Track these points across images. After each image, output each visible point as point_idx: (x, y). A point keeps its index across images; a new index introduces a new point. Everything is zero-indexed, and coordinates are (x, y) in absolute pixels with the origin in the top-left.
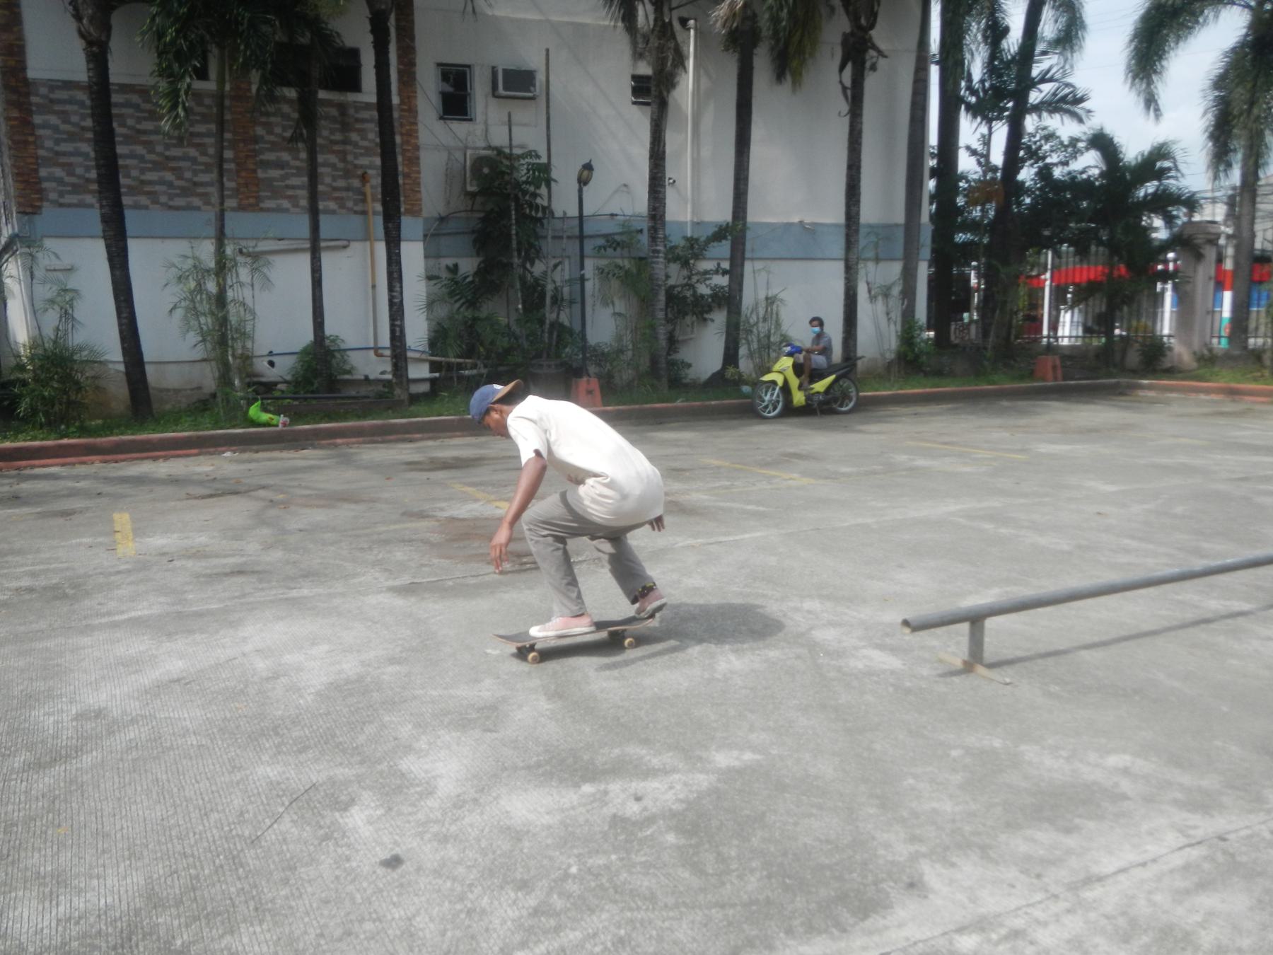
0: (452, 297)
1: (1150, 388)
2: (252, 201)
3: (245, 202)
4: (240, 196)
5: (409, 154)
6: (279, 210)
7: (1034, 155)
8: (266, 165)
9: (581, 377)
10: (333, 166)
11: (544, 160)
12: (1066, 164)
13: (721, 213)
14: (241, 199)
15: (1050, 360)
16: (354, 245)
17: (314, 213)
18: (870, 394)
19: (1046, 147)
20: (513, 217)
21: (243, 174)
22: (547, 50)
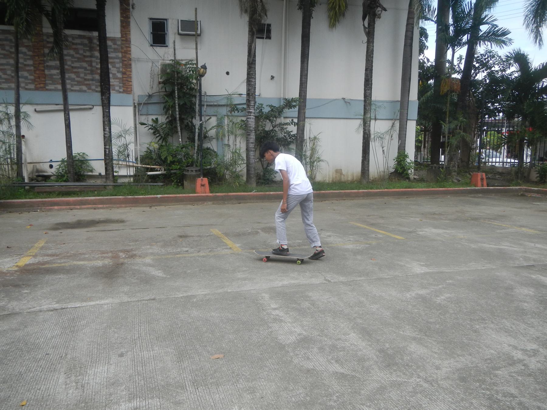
0: (155, 135)
1: (538, 192)
2: (42, 85)
3: (38, 86)
4: (36, 83)
5: (126, 63)
6: (56, 90)
7: (485, 65)
8: (50, 68)
9: (200, 177)
10: (85, 69)
11: (195, 66)
12: (504, 70)
13: (294, 93)
14: (36, 85)
15: (480, 175)
16: (94, 107)
17: (65, 91)
18: (366, 191)
19: (491, 62)
20: (176, 94)
21: (37, 72)
22: (196, 9)
